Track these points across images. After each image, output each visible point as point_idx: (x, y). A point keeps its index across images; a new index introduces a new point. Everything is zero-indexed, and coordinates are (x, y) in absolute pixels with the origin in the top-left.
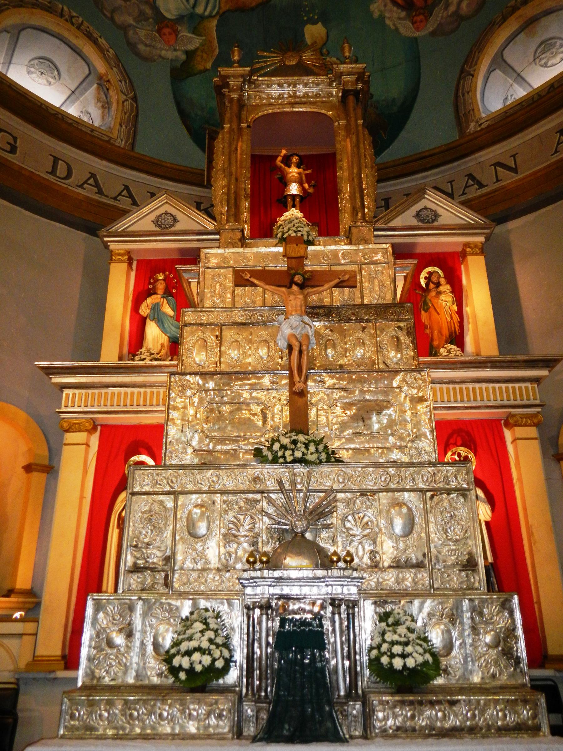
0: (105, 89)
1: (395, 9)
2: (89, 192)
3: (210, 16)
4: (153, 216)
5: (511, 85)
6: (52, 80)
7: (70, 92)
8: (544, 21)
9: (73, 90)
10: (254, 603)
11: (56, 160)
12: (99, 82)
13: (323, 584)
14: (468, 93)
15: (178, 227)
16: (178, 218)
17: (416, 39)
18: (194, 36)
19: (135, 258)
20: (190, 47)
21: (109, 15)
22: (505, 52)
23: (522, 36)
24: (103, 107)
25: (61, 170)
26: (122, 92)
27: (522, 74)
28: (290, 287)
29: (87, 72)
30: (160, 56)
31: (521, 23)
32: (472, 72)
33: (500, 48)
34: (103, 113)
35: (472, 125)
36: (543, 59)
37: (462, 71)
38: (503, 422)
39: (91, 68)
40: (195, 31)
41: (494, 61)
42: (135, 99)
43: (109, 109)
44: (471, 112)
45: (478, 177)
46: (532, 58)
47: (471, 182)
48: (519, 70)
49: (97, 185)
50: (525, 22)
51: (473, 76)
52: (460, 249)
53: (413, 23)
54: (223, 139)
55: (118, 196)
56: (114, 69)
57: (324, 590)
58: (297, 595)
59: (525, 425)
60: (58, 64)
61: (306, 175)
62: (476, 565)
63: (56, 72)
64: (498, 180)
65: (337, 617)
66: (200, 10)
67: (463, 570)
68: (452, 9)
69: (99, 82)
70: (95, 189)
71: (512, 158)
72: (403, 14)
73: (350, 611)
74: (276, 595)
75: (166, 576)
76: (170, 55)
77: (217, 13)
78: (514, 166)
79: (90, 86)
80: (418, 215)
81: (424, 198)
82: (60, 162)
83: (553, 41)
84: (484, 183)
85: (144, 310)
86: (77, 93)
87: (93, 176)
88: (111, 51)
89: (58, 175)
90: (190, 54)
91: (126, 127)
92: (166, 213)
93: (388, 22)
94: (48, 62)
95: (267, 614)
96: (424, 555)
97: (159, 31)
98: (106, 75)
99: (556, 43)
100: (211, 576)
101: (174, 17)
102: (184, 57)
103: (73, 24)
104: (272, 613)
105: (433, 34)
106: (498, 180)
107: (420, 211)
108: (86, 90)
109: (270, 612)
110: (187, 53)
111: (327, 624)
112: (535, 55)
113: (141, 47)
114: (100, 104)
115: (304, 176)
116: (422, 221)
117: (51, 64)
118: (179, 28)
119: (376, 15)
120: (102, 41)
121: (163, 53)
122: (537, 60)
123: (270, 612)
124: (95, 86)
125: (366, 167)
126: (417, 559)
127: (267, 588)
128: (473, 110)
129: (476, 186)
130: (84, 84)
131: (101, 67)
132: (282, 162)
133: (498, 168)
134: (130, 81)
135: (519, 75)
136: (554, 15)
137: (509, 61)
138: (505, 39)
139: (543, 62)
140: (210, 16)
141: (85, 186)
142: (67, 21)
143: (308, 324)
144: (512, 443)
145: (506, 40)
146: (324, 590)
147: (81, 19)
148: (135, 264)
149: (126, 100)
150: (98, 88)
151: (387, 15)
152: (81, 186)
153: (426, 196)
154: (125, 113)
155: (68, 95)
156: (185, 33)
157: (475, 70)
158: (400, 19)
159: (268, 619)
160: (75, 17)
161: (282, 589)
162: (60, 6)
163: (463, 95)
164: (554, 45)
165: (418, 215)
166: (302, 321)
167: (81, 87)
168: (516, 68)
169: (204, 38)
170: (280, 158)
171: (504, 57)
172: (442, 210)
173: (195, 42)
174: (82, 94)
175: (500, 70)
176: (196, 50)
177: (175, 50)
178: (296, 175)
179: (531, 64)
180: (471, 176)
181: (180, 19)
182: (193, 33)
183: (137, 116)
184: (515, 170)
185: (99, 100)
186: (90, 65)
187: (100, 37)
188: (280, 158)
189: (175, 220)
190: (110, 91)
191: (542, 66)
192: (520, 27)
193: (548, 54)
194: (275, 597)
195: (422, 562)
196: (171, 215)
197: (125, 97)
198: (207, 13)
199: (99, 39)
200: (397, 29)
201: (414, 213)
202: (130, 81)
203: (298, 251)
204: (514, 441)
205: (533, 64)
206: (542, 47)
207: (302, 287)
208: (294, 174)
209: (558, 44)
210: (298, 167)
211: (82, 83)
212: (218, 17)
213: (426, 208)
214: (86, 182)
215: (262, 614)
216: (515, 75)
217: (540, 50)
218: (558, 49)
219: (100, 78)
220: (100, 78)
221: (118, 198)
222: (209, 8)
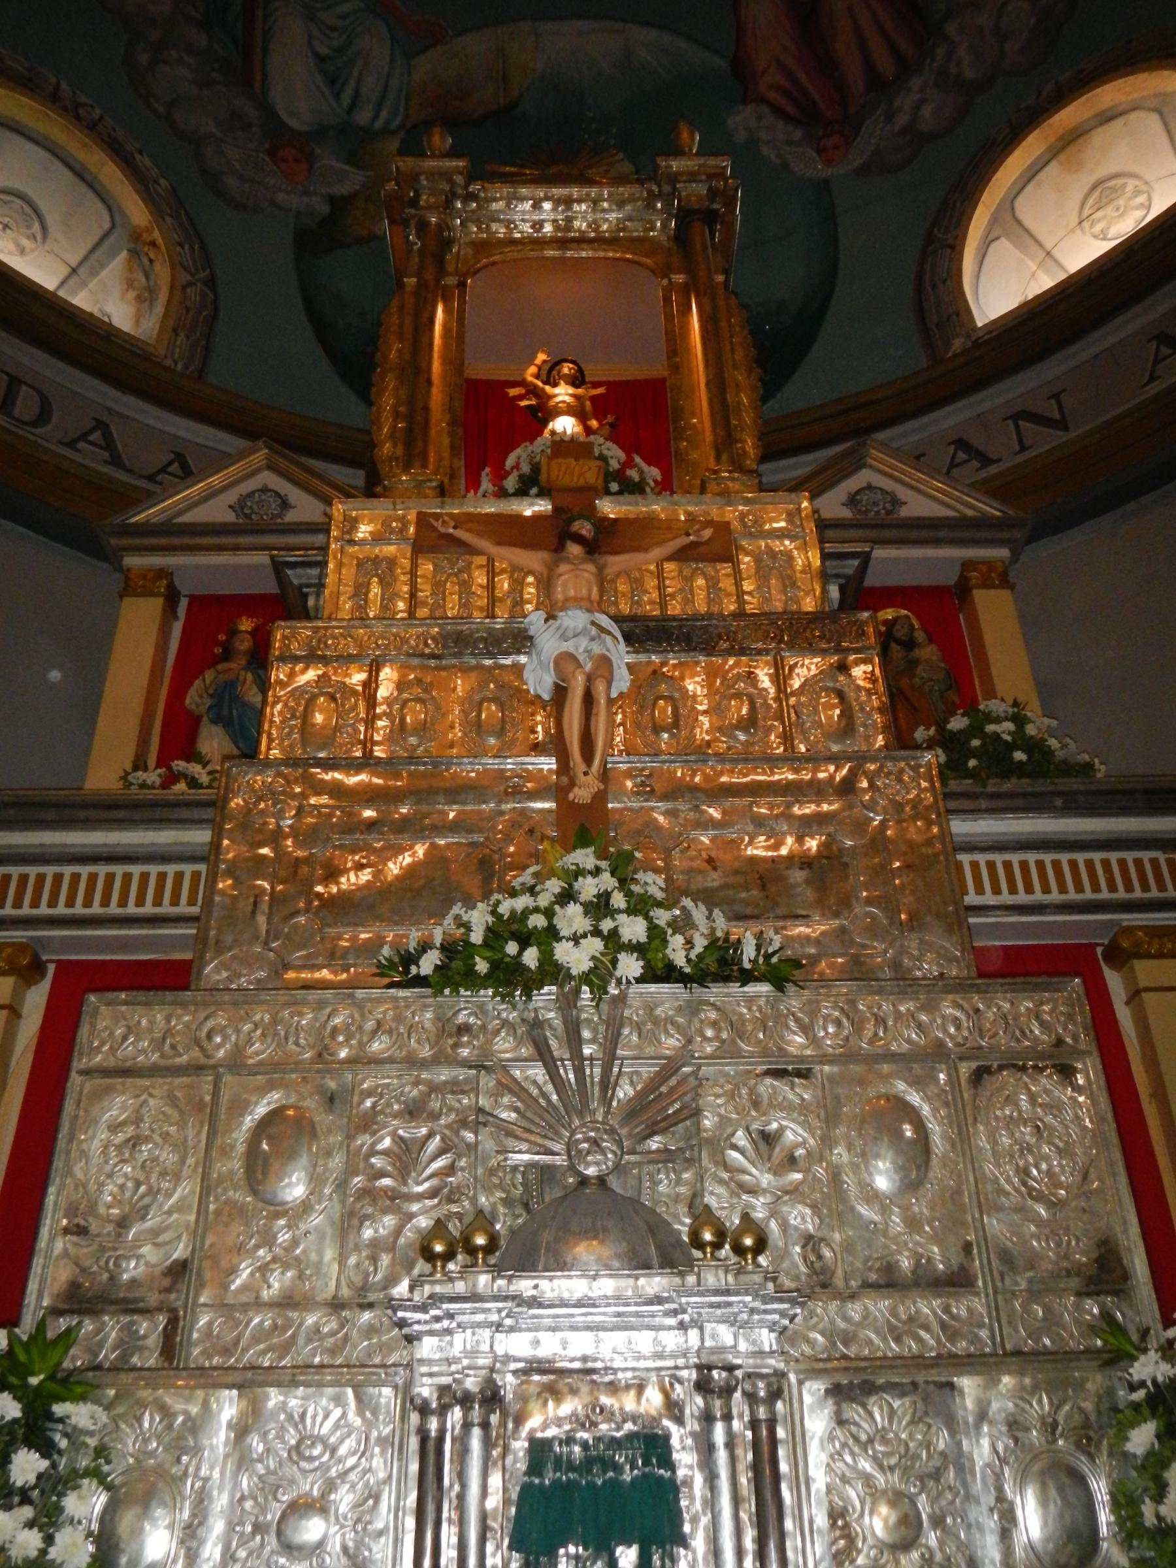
0: (146, 262)
1: (780, 124)
2: (90, 457)
3: (386, 132)
4: (232, 496)
5: (1033, 274)
6: (25, 242)
7: (67, 270)
8: (1099, 137)
9: (74, 264)
10: (443, 1390)
11: (14, 383)
12: (132, 246)
13: (671, 1321)
14: (944, 282)
15: (290, 517)
16: (292, 500)
17: (826, 181)
18: (347, 168)
19: (184, 590)
20: (342, 190)
21: (161, 110)
22: (1018, 203)
23: (1053, 169)
24: (139, 299)
25: (25, 405)
26: (181, 265)
27: (1055, 253)
28: (560, 548)
29: (107, 225)
30: (273, 203)
31: (1052, 139)
32: (951, 241)
33: (1006, 193)
34: (138, 310)
36: (1099, 220)
37: (929, 239)
38: (1099, 950)
39: (117, 218)
40: (352, 159)
41: (995, 219)
42: (211, 282)
43: (152, 301)
44: (954, 318)
45: (978, 442)
46: (1076, 221)
47: (962, 456)
48: (1049, 245)
49: (109, 444)
50: (1060, 139)
51: (952, 247)
52: (949, 578)
53: (820, 151)
54: (402, 307)
55: (158, 473)
56: (168, 219)
57: (671, 1340)
58: (584, 1359)
59: (1160, 955)
60: (42, 205)
61: (593, 399)
62: (1126, 1276)
63: (36, 226)
64: (1023, 448)
65: (719, 1433)
66: (363, 117)
67: (1089, 1295)
68: (902, 120)
69: (132, 246)
70: (106, 455)
71: (1053, 401)
72: (798, 134)
73: (762, 1413)
74: (517, 1360)
75: (173, 1322)
76: (295, 202)
77: (400, 128)
78: (1057, 416)
79: (113, 255)
81: (865, 466)
82: (24, 388)
83: (1119, 181)
84: (994, 456)
85: (195, 698)
86: (81, 271)
87: (101, 425)
88: (162, 181)
89: (16, 413)
90: (339, 205)
91: (188, 337)
92: (265, 490)
93: (765, 150)
94: (18, 201)
95: (485, 1425)
96: (967, 1248)
97: (272, 153)
98: (148, 230)
99: (1125, 185)
100: (310, 1320)
101: (306, 128)
102: (325, 209)
103: (78, 118)
104: (503, 1424)
105: (863, 171)
106: (1023, 448)
107: (858, 492)
108: (103, 266)
109: (494, 1419)
110: (333, 200)
111: (685, 1460)
112: (1080, 213)
113: (231, 182)
114: (131, 295)
115: (588, 403)
117: (27, 209)
118: (318, 151)
119: (741, 137)
120: (143, 161)
121: (281, 197)
122: (1086, 224)
123: (494, 1419)
124: (124, 254)
125: (735, 367)
126: (946, 1260)
127: (486, 1333)
128: (958, 315)
129: (975, 464)
130: (98, 254)
131: (137, 212)
133: (1021, 423)
134: (203, 247)
135: (1048, 253)
136: (1119, 122)
137: (1028, 221)
138: (1017, 174)
139: (1098, 228)
140: (386, 132)
141: (81, 445)
142: (66, 110)
143: (610, 633)
144: (1127, 1003)
145: (1022, 175)
146: (671, 1340)
147: (97, 112)
148: (183, 604)
149: (190, 284)
150: (130, 260)
151: (764, 136)
152: (71, 444)
153: (870, 461)
154: (188, 310)
155: (62, 277)
156: (328, 160)
157: (956, 237)
158: (790, 143)
159: (488, 1444)
160: (83, 105)
161: (536, 1343)
162: (53, 80)
163: (934, 287)
164: (1118, 191)
165: (852, 500)
166: (593, 623)
167: (94, 257)
168: (1041, 238)
169: (370, 173)
170: (533, 369)
171: (1018, 213)
172: (911, 493)
173: (350, 181)
174: (94, 273)
175: (1008, 238)
176: (353, 196)
177: (307, 193)
179: (1072, 231)
180: (962, 444)
181: (320, 133)
182: (348, 162)
183: (214, 317)
184: (1062, 424)
185: (130, 284)
186: (115, 209)
187: (141, 152)
189: (285, 505)
190: (157, 266)
191: (1096, 237)
192: (1050, 148)
193: (1109, 211)
194: (513, 1366)
195: (962, 1268)
196: (277, 493)
197: (189, 277)
198: (379, 124)
199: (138, 157)
200: (786, 166)
201: (844, 498)
202: (203, 247)
203: (581, 475)
204: (1135, 996)
205: (1078, 231)
206: (1097, 193)
207: (593, 548)
208: (567, 399)
209: (1130, 188)
211: (92, 251)
212: (402, 134)
213: (869, 487)
214: (83, 437)
215: (467, 1426)
217: (1091, 201)
218: (1131, 199)
219: (136, 236)
220: (136, 236)
221: (159, 478)
222: (384, 114)
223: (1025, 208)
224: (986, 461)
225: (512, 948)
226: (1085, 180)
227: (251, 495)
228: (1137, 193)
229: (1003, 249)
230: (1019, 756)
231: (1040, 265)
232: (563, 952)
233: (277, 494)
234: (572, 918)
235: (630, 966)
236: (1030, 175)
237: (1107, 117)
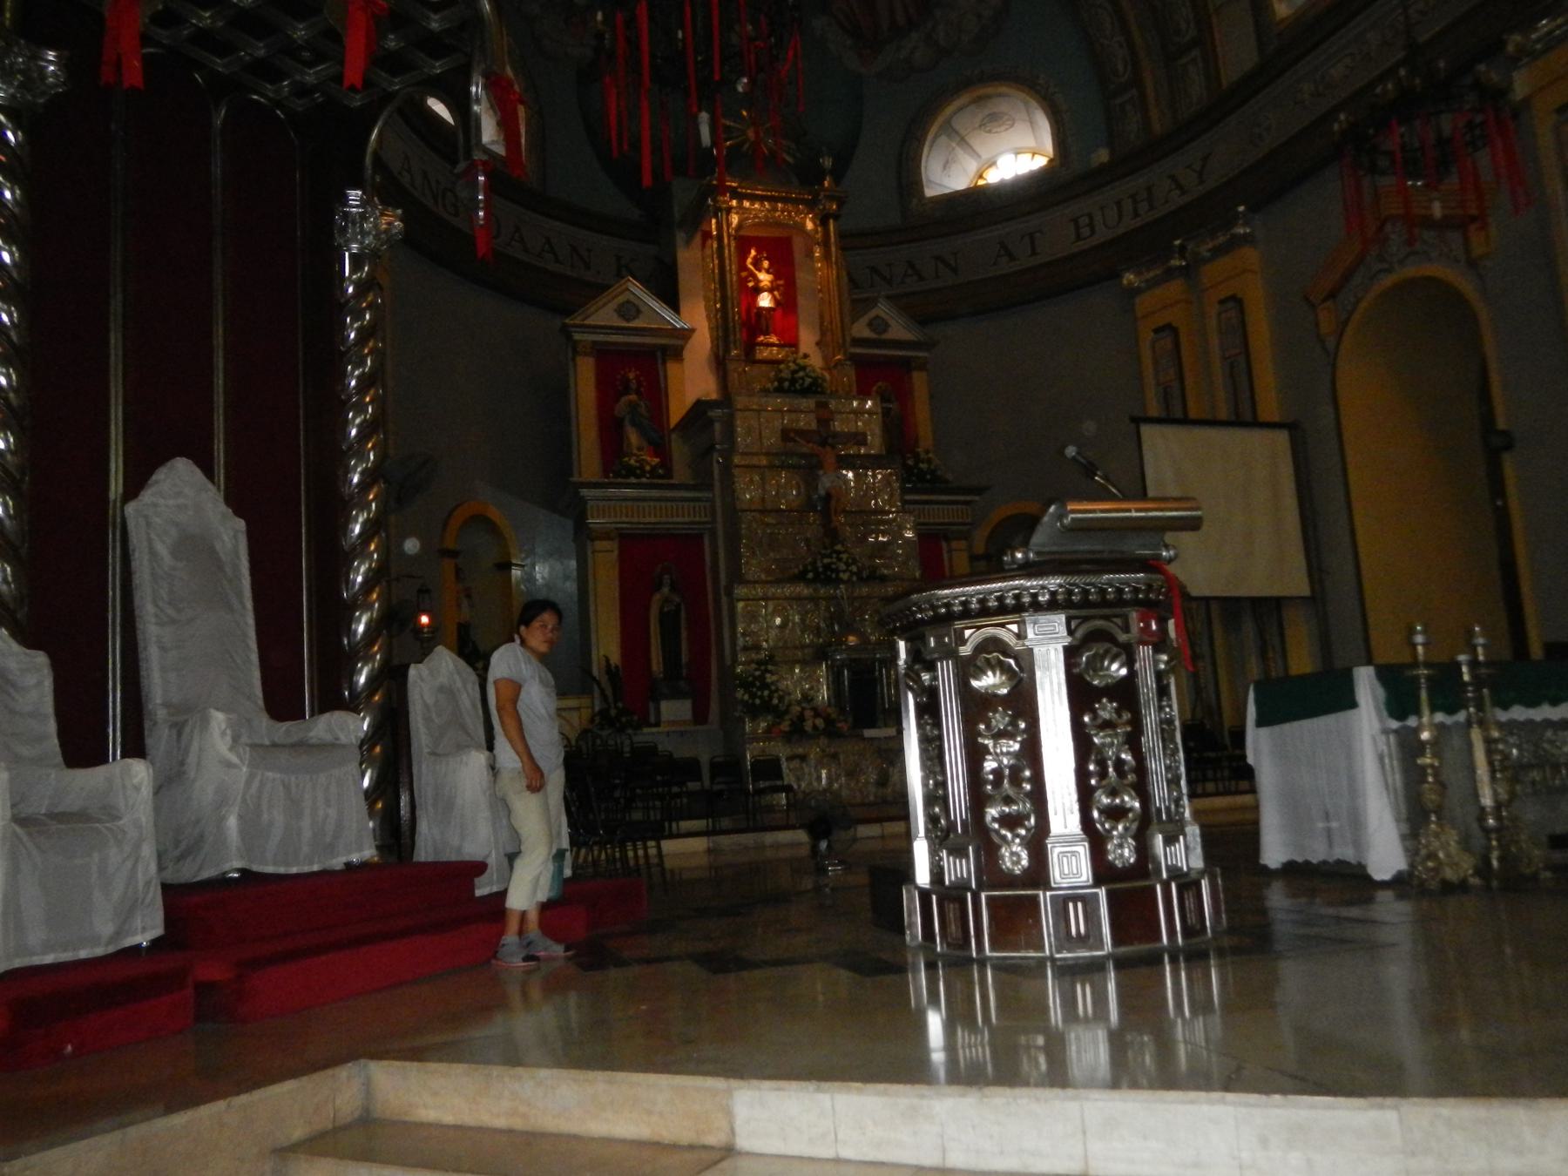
5: (953, 149)
35: (915, 201)
41: (941, 127)
47: (910, 272)
80: (870, 324)
92: (628, 302)
116: (874, 330)
132: (752, 264)
139: (988, 129)
178: (769, 284)
184: (955, 270)
188: (749, 260)
204: (950, 551)
210: (768, 272)
213: (877, 317)
216: (958, 139)
223: (958, 123)
224: (921, 278)
225: (829, 573)
226: (987, 112)
227: (622, 305)
228: (1008, 120)
229: (943, 139)
230: (928, 477)
231: (958, 144)
232: (841, 575)
233: (634, 304)
234: (842, 566)
235: (855, 578)
236: (960, 109)
237: (1000, 95)
